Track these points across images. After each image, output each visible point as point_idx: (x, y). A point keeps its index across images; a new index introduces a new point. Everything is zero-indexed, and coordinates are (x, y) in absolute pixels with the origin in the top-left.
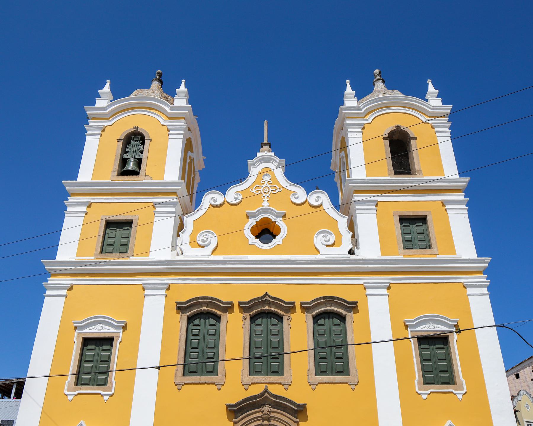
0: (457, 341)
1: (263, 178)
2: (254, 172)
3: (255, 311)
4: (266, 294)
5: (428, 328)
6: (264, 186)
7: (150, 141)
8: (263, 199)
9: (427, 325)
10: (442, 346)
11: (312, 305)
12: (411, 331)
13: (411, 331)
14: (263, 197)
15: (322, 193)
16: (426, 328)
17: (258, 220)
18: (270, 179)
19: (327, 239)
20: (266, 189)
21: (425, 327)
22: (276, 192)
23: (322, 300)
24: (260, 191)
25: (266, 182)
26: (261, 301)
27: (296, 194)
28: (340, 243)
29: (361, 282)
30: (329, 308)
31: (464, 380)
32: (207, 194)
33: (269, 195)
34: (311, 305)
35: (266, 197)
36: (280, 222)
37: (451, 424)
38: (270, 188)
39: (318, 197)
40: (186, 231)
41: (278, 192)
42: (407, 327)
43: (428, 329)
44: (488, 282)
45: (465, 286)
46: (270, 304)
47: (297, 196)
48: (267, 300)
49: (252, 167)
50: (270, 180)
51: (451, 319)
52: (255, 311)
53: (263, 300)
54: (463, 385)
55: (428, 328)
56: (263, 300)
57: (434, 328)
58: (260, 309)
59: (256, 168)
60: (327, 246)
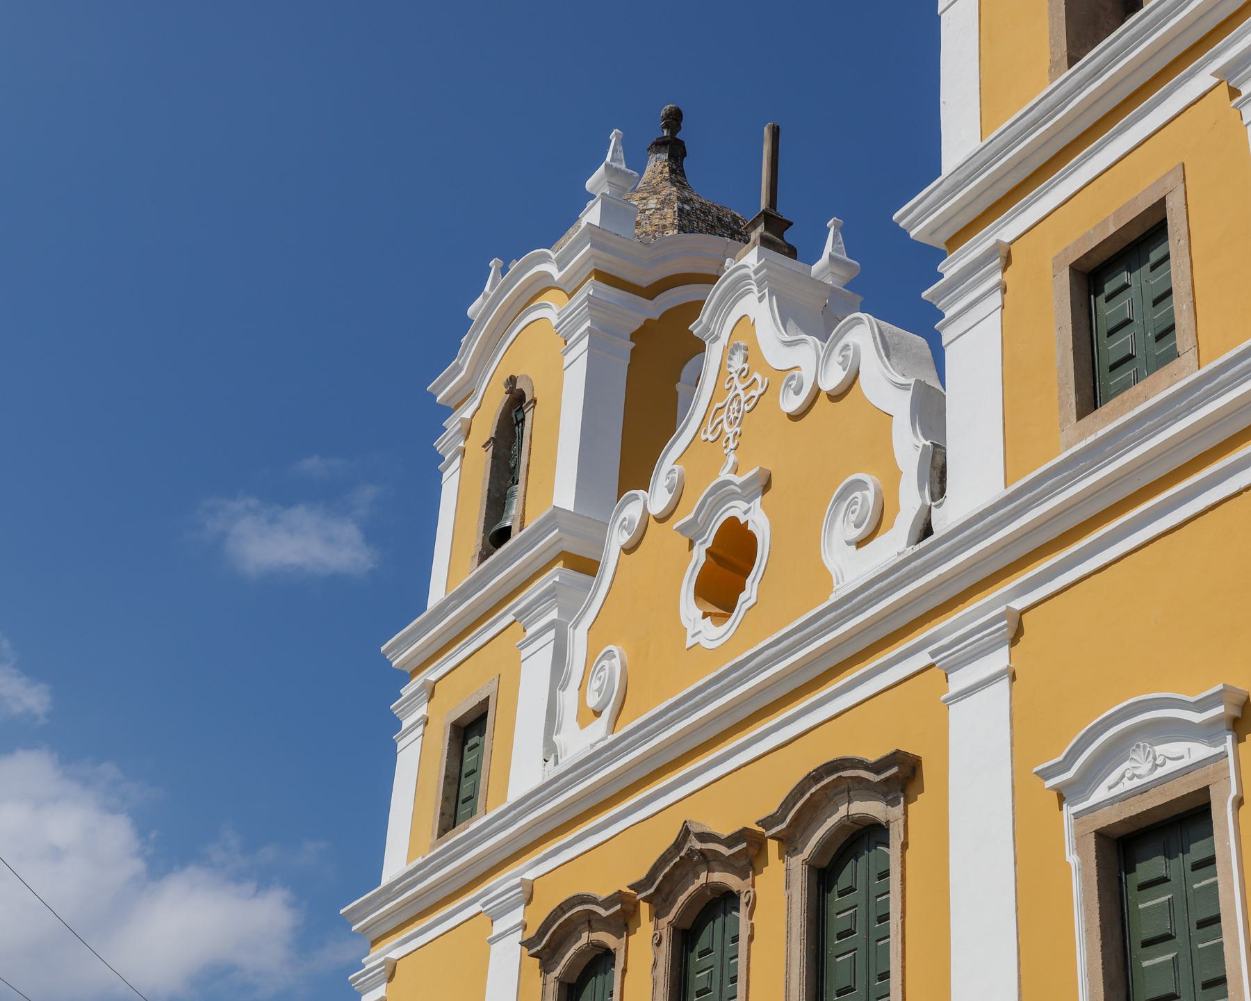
1: (730, 366)
2: (714, 354)
3: (682, 899)
4: (685, 832)
5: (1134, 776)
6: (731, 395)
7: (534, 407)
8: (726, 451)
9: (1127, 764)
11: (788, 820)
14: (726, 443)
15: (847, 326)
16: (1125, 780)
17: (709, 544)
18: (742, 359)
19: (853, 517)
20: (735, 405)
21: (1123, 776)
22: (754, 400)
23: (813, 790)
24: (720, 426)
25: (735, 376)
26: (677, 859)
27: (793, 377)
28: (897, 509)
29: (922, 659)
30: (842, 811)
32: (614, 518)
33: (739, 426)
34: (784, 826)
35: (731, 436)
36: (757, 519)
38: (742, 393)
39: (846, 347)
40: (572, 675)
41: (761, 395)
43: (1137, 782)
46: (707, 860)
47: (794, 383)
48: (692, 851)
49: (707, 343)
50: (746, 360)
52: (682, 899)
53: (682, 854)
55: (1134, 776)
56: (682, 854)
58: (692, 888)
59: (717, 338)
60: (860, 543)
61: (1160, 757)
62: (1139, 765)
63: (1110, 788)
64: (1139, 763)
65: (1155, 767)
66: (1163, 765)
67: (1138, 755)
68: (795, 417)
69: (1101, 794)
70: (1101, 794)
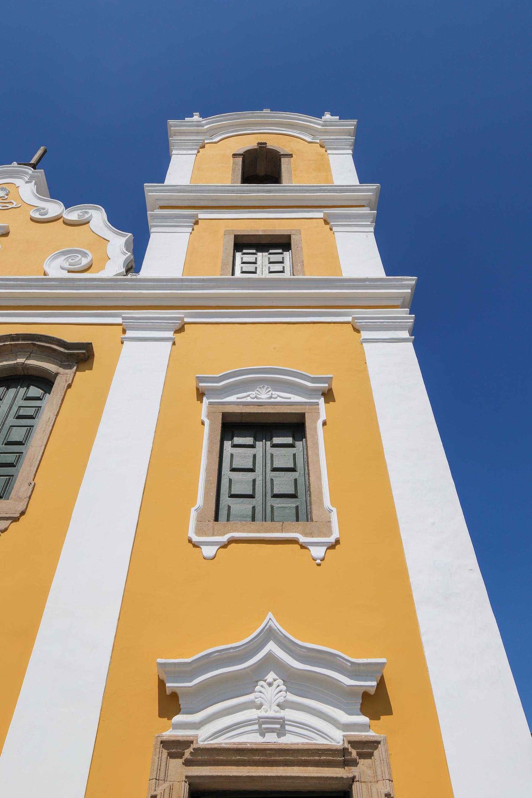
0: (324, 424)
5: (256, 397)
9: (254, 393)
10: (289, 440)
12: (210, 404)
13: (210, 404)
21: (248, 396)
31: (335, 510)
37: (270, 626)
42: (200, 395)
44: (410, 320)
45: (357, 327)
51: (312, 376)
54: (330, 522)
55: (256, 397)
57: (271, 397)
61: (275, 395)
62: (260, 394)
63: (237, 398)
64: (261, 394)
65: (271, 397)
66: (276, 398)
67: (262, 390)
68: (33, 220)
69: (233, 398)
70: (233, 398)
